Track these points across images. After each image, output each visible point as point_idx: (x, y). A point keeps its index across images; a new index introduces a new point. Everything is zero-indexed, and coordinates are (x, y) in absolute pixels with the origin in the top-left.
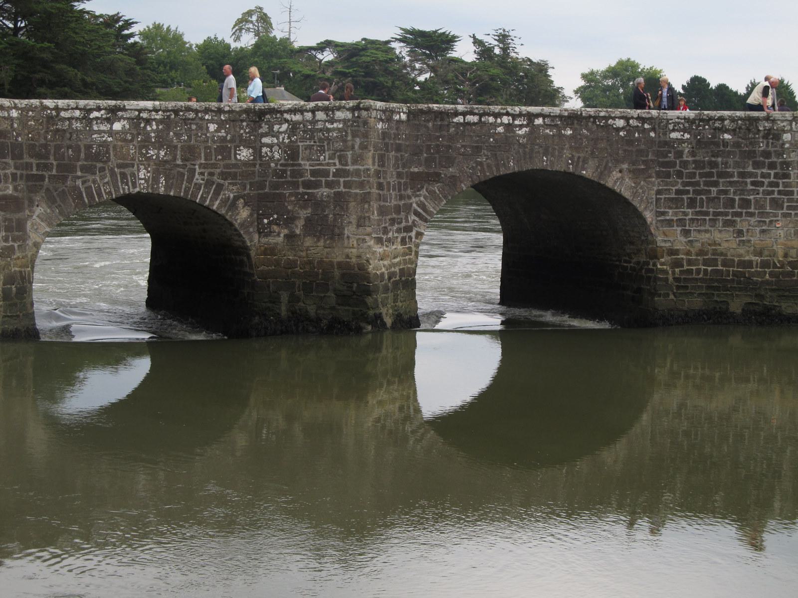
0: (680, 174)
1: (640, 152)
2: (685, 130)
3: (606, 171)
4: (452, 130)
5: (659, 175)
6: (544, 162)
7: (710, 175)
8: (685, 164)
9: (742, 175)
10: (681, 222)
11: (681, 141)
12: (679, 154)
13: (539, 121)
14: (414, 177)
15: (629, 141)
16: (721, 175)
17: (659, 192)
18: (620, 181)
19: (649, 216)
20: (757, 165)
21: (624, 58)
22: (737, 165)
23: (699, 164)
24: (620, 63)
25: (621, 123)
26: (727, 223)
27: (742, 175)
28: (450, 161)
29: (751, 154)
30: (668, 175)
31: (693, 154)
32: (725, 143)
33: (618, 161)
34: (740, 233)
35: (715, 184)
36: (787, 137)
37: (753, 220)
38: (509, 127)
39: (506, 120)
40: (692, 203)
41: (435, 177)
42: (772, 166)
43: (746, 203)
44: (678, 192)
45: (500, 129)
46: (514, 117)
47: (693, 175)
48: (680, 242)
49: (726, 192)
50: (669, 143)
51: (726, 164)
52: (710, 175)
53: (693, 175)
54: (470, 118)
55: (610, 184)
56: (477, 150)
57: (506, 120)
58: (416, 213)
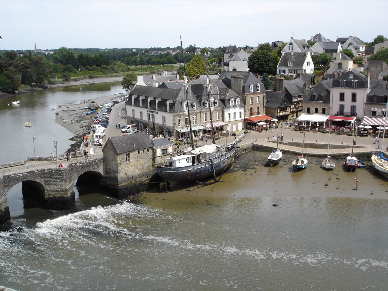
0: (47, 178)
1: (41, 175)
2: (47, 171)
3: (35, 179)
4: (10, 178)
5: (44, 178)
6: (26, 180)
7: (52, 177)
8: (48, 176)
9: (57, 177)
10: (48, 185)
11: (47, 173)
12: (47, 175)
13: (24, 174)
14: (5, 186)
15: (39, 174)
16: (53, 177)
17: (44, 180)
18: (38, 180)
19: (43, 184)
20: (59, 176)
21: (63, 46)
22: (56, 176)
23: (50, 176)
24: (62, 47)
25: (37, 171)
26: (56, 184)
27: (57, 177)
28: (10, 183)
29: (58, 174)
30: (45, 178)
31: (49, 175)
32: (54, 173)
33: (37, 177)
34: (57, 186)
35: (53, 179)
36: (63, 171)
37: (59, 184)
38: (19, 176)
39: (18, 175)
40: (49, 182)
41: (8, 185)
42: (61, 176)
43: (57, 181)
44: (47, 180)
45: (18, 176)
46: (20, 174)
47: (49, 178)
48: (48, 188)
49: (54, 180)
50: (45, 173)
51: (54, 176)
52: (52, 177)
53: (49, 178)
54: (13, 175)
55: (36, 181)
56: (15, 180)
57: (18, 175)
58: (6, 191)
